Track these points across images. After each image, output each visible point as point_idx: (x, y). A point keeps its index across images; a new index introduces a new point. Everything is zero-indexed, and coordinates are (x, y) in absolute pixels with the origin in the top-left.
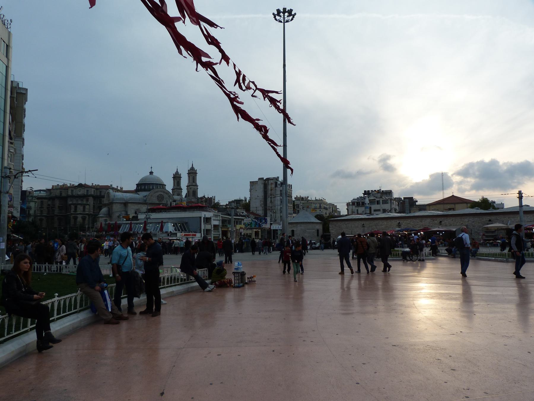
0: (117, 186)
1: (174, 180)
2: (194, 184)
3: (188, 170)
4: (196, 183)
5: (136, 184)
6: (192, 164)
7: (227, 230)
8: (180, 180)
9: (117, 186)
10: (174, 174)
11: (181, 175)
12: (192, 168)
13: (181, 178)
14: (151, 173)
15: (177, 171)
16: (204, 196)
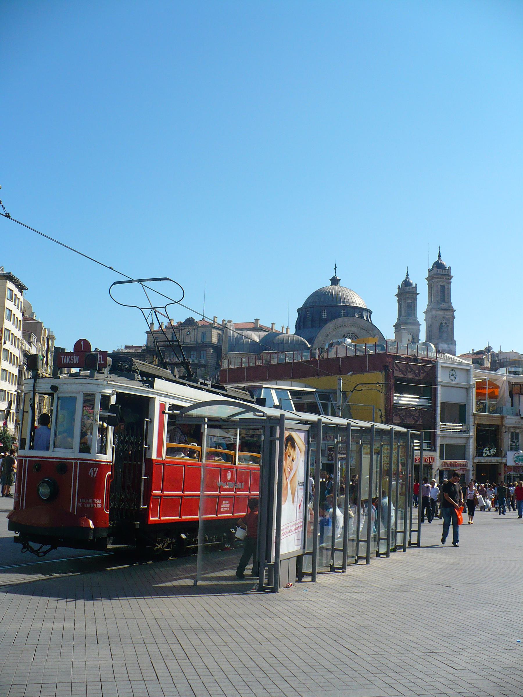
0: (273, 324)
1: (399, 301)
2: (444, 305)
3: (429, 269)
4: (449, 302)
5: (298, 311)
6: (439, 252)
7: (499, 423)
8: (415, 299)
9: (273, 324)
10: (399, 286)
11: (416, 287)
12: (438, 265)
13: (418, 296)
14: (335, 281)
15: (407, 278)
16: (488, 349)
